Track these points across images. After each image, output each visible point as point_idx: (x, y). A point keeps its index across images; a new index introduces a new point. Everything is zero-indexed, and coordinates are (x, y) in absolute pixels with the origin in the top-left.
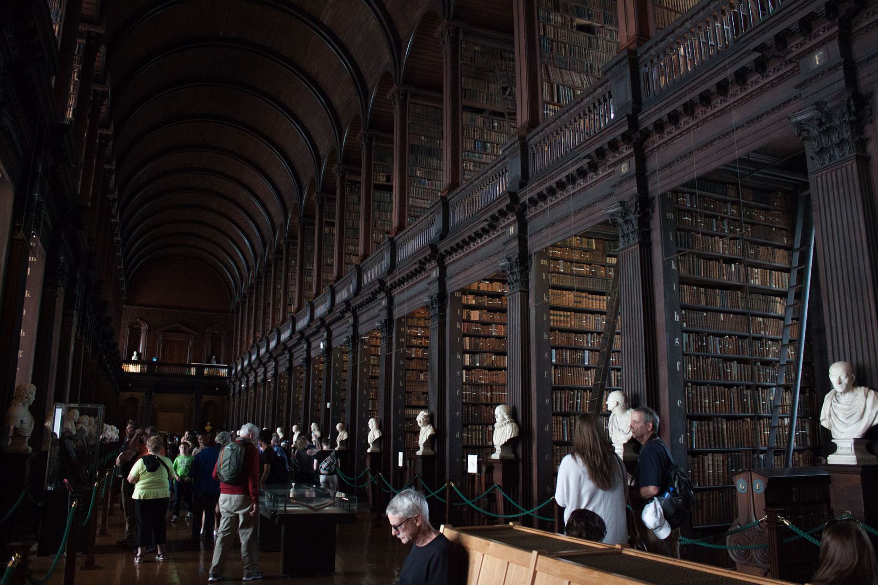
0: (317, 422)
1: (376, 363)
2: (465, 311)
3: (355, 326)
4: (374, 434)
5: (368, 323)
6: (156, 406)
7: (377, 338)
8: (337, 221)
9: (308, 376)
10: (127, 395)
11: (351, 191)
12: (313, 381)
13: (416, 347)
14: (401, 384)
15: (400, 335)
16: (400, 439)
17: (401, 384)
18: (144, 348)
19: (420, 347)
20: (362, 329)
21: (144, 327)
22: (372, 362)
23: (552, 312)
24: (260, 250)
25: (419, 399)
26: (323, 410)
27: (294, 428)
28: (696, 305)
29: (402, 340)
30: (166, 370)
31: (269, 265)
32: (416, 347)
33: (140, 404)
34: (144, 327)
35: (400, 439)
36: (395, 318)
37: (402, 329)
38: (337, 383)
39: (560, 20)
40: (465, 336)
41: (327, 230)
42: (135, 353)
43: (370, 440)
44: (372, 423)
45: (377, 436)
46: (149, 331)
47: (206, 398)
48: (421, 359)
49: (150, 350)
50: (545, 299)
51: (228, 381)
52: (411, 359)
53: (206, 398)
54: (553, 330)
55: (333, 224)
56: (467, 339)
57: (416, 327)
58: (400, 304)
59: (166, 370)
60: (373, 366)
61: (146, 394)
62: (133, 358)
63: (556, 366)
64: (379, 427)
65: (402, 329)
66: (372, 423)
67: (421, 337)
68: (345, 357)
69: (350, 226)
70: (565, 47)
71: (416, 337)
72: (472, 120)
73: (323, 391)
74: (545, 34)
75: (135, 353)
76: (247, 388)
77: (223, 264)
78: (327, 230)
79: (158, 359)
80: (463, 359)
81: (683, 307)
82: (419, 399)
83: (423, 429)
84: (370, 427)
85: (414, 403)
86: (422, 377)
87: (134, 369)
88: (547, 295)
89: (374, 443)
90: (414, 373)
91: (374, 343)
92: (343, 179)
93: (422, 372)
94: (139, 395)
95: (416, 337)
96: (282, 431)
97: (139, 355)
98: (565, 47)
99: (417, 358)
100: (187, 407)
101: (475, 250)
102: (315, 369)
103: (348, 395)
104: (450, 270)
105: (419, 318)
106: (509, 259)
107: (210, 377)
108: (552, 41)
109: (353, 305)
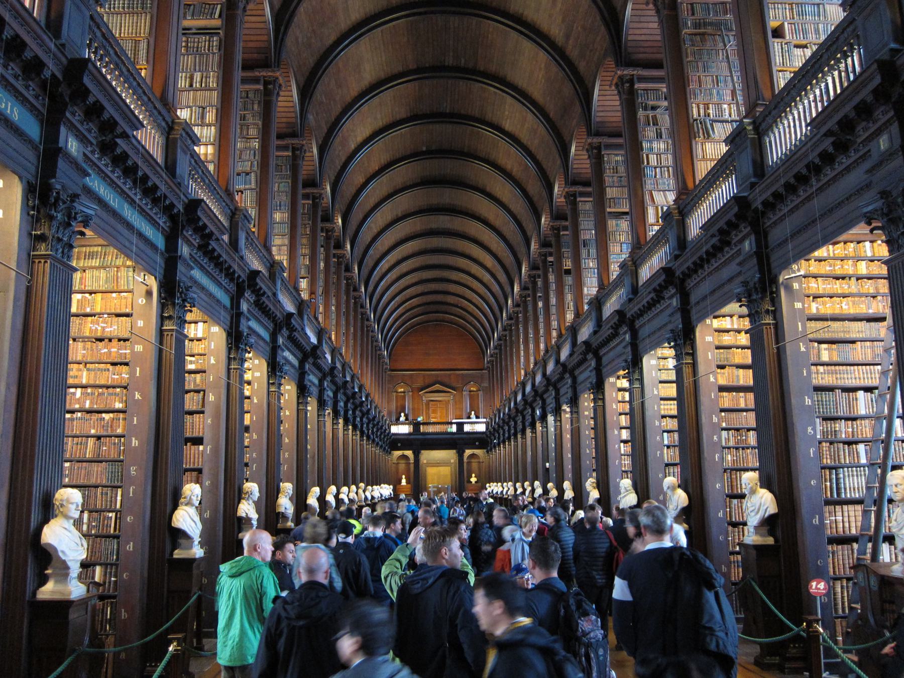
2: (620, 393)
23: (662, 402)
28: (736, 407)
39: (662, 146)
40: (621, 414)
50: (656, 392)
54: (664, 417)
56: (623, 417)
58: (582, 382)
63: (668, 447)
70: (668, 171)
72: (617, 225)
74: (648, 163)
80: (620, 434)
81: (722, 410)
83: (591, 494)
88: (657, 389)
94: (409, 453)
98: (668, 171)
100: (452, 461)
101: (614, 348)
104: (605, 360)
106: (626, 361)
108: (655, 168)
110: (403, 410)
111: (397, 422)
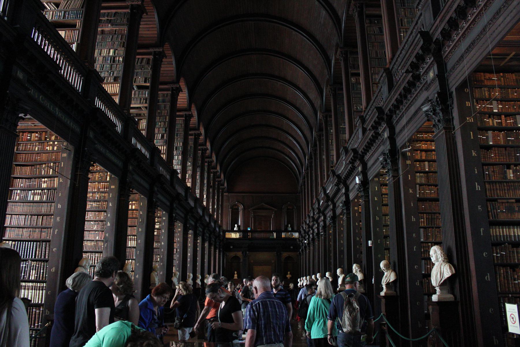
0: (359, 262)
1: (423, 181)
3: (392, 139)
4: (440, 270)
5: (409, 126)
6: (252, 261)
7: (422, 151)
8: (361, 71)
9: (348, 219)
10: (232, 254)
11: (371, 23)
12: (354, 223)
13: (493, 129)
14: (478, 188)
15: (464, 113)
16: (488, 278)
17: (478, 188)
18: (242, 222)
19: (500, 130)
20: (400, 141)
21: (241, 207)
22: (418, 181)
24: (308, 135)
25: (511, 210)
26: (364, 249)
27: (338, 271)
29: (470, 120)
30: (256, 235)
31: (315, 145)
32: (493, 129)
33: (241, 261)
34: (241, 207)
35: (488, 278)
36: (453, 90)
37: (468, 104)
38: (377, 218)
41: (353, 80)
42: (236, 225)
43: (435, 280)
44: (435, 253)
45: (447, 272)
46: (244, 209)
47: (285, 254)
48: (505, 147)
49: (246, 223)
51: (298, 240)
52: (488, 148)
53: (285, 254)
55: (358, 75)
57: (489, 100)
59: (256, 235)
60: (421, 185)
61: (243, 253)
62: (235, 229)
64: (449, 258)
65: (468, 104)
66: (435, 253)
67: (498, 115)
68: (384, 190)
69: (374, 55)
71: (491, 115)
73: (363, 233)
75: (236, 225)
76: (309, 243)
77: (288, 157)
78: (353, 80)
79: (251, 229)
82: (511, 210)
84: (433, 259)
85: (503, 217)
86: (511, 175)
87: (234, 236)
89: (442, 285)
90: (497, 168)
91: (418, 157)
92: (361, 14)
93: (508, 167)
94: (240, 254)
95: (491, 115)
96: (330, 275)
97: (238, 226)
99: (497, 146)
100: (273, 262)
102: (355, 212)
103: (391, 232)
105: (492, 88)
107: (286, 239)
109: (386, 111)
110: (237, 223)
111: (232, 231)
